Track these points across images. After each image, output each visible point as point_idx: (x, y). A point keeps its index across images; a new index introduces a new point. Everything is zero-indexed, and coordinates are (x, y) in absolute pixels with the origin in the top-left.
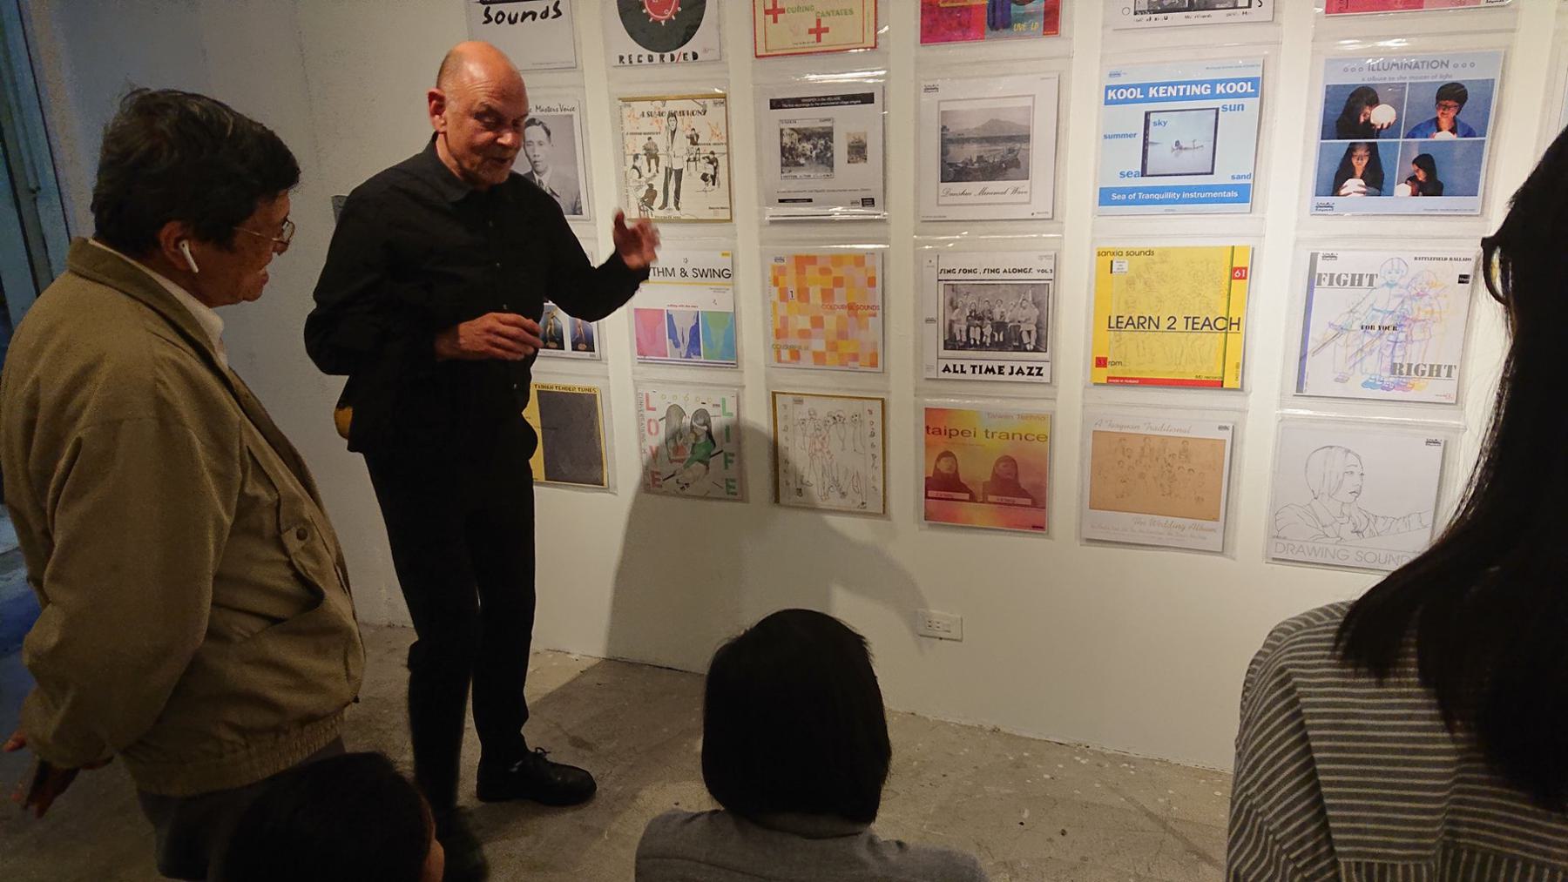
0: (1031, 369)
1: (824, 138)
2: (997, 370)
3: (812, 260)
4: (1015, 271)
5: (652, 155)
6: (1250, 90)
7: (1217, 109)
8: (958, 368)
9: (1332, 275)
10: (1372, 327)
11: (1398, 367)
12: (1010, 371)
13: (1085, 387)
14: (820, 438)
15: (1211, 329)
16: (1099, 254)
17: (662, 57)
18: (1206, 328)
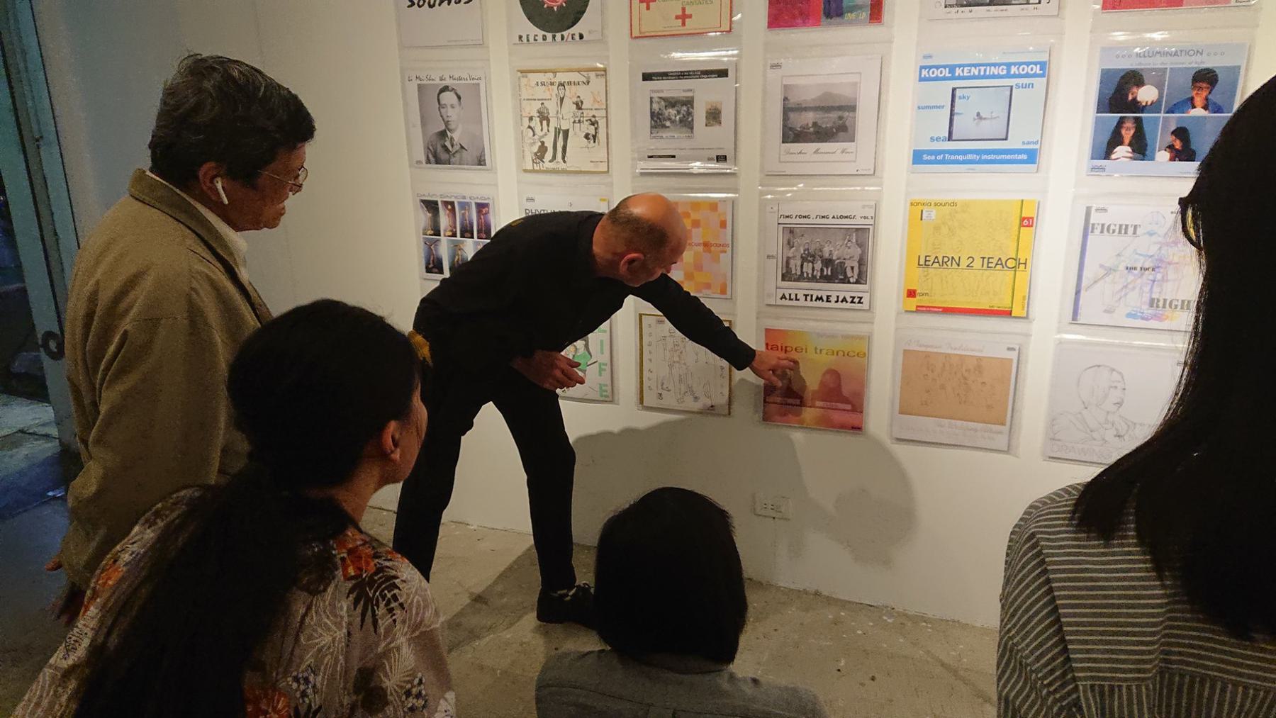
0: (854, 298)
1: (686, 105)
2: (825, 298)
4: (842, 217)
5: (544, 117)
6: (1038, 72)
7: (1012, 87)
8: (793, 297)
9: (1103, 225)
10: (1135, 269)
11: (1156, 301)
12: (836, 299)
13: (898, 314)
14: (678, 353)
15: (1003, 267)
16: (912, 204)
17: (554, 37)
18: (999, 267)
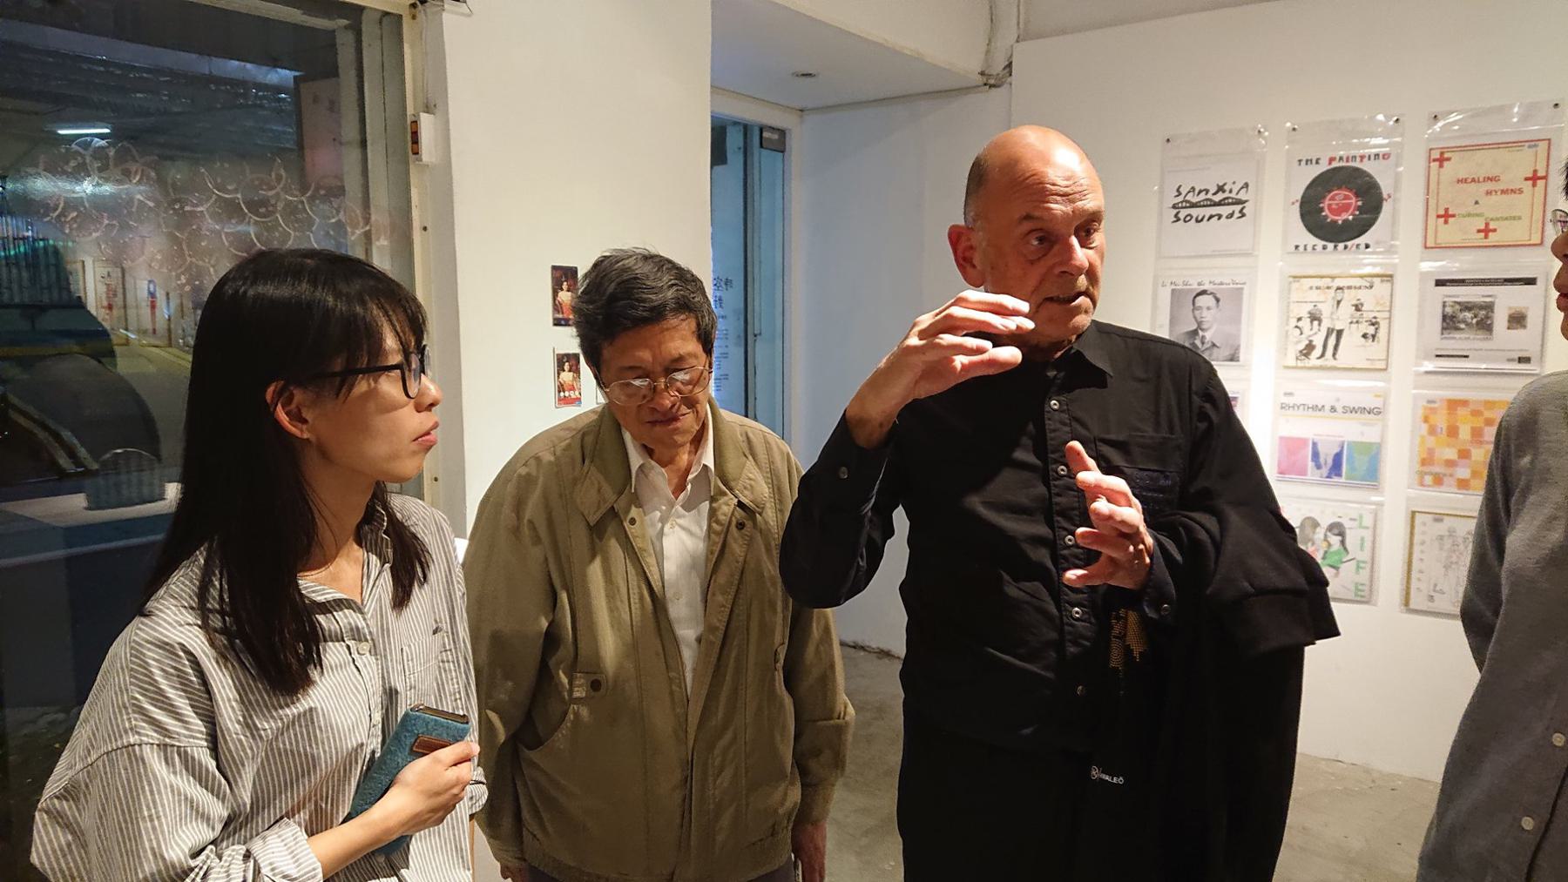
3: (1465, 403)
17: (1335, 247)
